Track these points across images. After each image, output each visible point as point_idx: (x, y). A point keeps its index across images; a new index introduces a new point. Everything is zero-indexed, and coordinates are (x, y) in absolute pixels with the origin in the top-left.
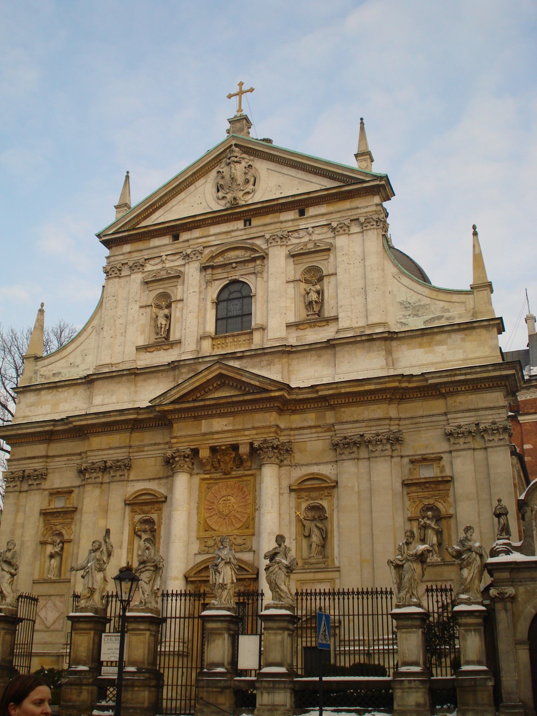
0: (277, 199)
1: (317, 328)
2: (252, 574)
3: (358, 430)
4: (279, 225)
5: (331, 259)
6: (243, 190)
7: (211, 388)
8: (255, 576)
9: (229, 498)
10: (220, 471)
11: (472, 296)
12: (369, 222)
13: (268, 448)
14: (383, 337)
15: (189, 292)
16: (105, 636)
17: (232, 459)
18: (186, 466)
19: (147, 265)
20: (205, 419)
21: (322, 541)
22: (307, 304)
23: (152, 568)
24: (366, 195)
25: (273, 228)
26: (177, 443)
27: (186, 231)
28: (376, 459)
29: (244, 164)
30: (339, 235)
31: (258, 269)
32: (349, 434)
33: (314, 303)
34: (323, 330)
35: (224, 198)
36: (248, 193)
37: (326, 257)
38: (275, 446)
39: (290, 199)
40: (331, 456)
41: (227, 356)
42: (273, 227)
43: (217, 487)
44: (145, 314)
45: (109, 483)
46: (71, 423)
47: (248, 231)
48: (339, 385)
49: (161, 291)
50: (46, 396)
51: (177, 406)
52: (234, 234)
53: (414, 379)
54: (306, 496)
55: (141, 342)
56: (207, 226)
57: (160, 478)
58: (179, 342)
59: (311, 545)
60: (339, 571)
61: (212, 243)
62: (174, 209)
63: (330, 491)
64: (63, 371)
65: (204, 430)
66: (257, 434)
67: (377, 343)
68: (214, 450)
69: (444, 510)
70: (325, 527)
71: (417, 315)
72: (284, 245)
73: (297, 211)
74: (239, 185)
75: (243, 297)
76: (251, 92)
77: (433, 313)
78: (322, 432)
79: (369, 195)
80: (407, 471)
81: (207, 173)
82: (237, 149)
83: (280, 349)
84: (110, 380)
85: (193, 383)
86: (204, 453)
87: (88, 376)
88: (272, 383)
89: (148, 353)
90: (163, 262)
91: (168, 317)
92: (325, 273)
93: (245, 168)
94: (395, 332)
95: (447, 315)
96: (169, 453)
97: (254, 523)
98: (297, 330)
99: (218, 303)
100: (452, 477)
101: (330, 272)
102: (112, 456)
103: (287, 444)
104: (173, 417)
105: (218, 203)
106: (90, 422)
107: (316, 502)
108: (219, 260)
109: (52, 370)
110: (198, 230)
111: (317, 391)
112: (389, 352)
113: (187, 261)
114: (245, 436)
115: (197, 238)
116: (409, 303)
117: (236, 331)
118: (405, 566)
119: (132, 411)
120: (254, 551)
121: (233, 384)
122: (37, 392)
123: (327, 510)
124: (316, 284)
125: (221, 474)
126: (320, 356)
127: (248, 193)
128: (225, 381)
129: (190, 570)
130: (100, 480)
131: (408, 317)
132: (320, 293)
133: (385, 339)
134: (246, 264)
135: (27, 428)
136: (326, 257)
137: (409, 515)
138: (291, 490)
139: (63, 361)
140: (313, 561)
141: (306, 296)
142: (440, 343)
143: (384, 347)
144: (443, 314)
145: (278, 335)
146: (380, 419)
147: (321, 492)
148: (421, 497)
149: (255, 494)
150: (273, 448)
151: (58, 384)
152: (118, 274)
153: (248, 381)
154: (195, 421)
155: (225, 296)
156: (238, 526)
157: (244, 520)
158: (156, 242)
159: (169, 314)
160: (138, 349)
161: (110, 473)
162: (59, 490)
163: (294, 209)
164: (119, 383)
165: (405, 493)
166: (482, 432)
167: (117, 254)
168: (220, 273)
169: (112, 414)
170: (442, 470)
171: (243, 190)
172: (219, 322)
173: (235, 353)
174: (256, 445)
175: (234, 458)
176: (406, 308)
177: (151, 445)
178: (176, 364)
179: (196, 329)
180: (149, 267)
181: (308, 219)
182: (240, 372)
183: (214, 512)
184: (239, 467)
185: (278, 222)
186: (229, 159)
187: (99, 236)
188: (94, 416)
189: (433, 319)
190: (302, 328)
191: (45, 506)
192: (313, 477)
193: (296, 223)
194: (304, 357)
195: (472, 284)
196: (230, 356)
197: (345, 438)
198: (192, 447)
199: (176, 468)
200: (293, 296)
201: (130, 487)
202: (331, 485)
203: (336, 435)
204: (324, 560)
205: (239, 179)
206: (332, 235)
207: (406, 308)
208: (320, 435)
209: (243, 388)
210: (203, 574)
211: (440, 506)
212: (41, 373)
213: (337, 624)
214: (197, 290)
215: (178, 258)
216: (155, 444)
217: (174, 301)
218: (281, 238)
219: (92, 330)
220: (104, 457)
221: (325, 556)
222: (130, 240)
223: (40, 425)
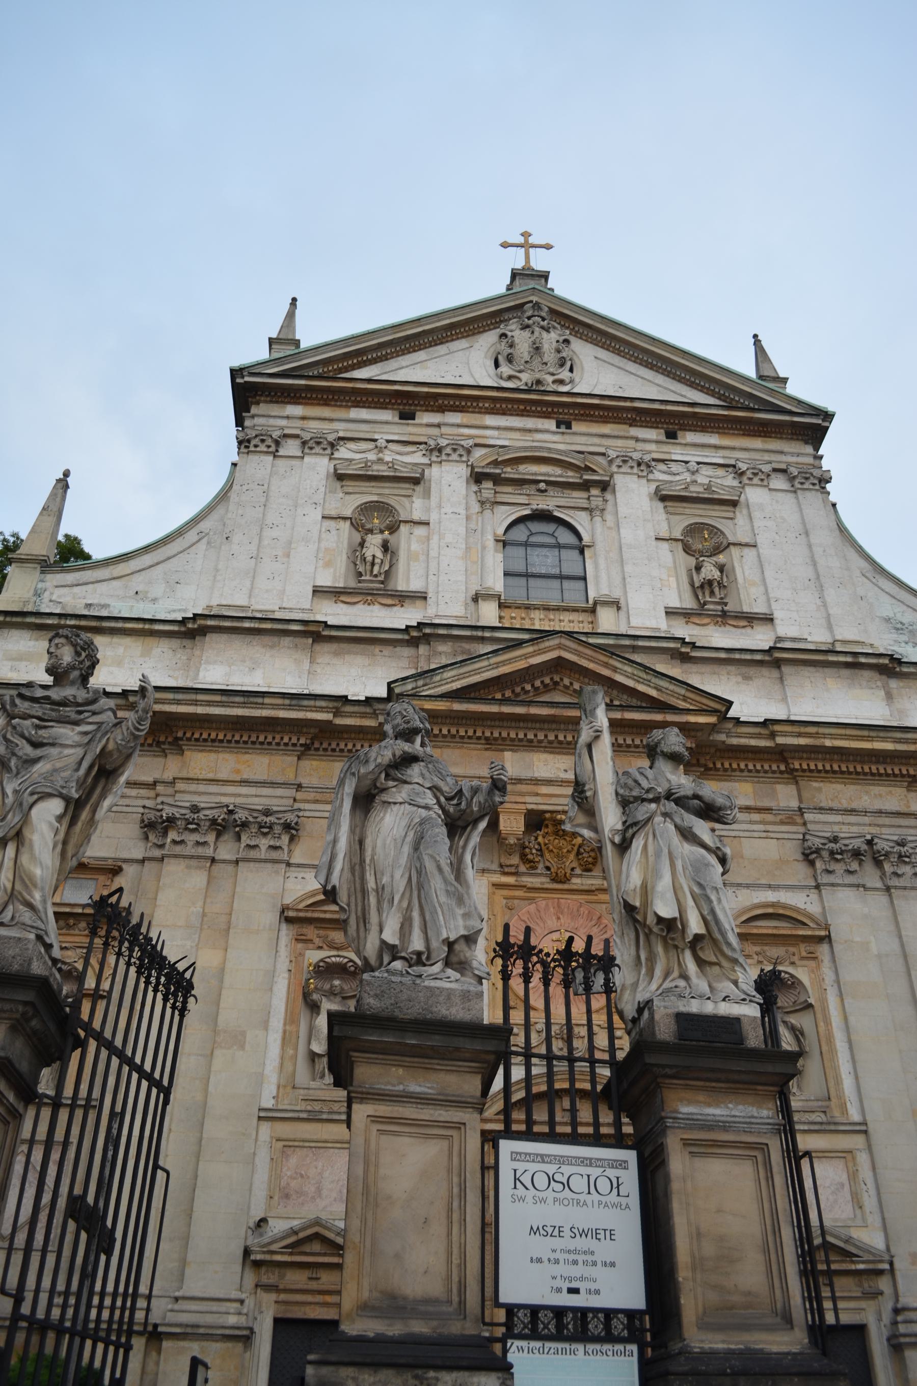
1: (728, 628)
3: (855, 829)
4: (631, 443)
7: (528, 687)
10: (541, 869)
15: (443, 511)
17: (576, 848)
19: (342, 449)
20: (511, 750)
22: (697, 584)
24: (792, 439)
25: (620, 445)
27: (433, 411)
28: (906, 893)
29: (554, 336)
30: (753, 485)
31: (596, 502)
33: (716, 584)
34: (742, 634)
35: (510, 378)
37: (731, 515)
39: (656, 406)
40: (800, 873)
42: (619, 443)
43: (532, 907)
44: (334, 532)
47: (568, 438)
48: (822, 730)
49: (375, 498)
51: (457, 706)
55: (326, 580)
60: (865, 1132)
61: (492, 442)
63: (812, 949)
67: (867, 674)
73: (662, 431)
74: (546, 364)
79: (798, 439)
81: (474, 334)
83: (672, 645)
84: (249, 638)
90: (380, 450)
92: (731, 539)
98: (687, 623)
106: (200, 710)
108: (509, 472)
110: (459, 414)
111: (773, 735)
112: (889, 696)
113: (434, 459)
115: (459, 426)
116: (901, 623)
119: (323, 703)
125: (544, 879)
126: (747, 678)
127: (561, 382)
130: (209, 852)
131: (903, 645)
133: (883, 670)
136: (731, 515)
141: (694, 571)
147: (792, 949)
151: (106, 624)
152: (273, 449)
153: (630, 683)
154: (486, 749)
160: (318, 592)
163: (657, 428)
164: (272, 647)
167: (273, 414)
168: (508, 494)
169: (267, 700)
175: (580, 846)
176: (898, 629)
178: (427, 631)
180: (343, 452)
181: (688, 448)
182: (612, 662)
184: (589, 870)
185: (632, 438)
186: (529, 318)
187: (235, 373)
188: (218, 698)
190: (698, 622)
193: (665, 448)
194: (714, 673)
197: (835, 840)
200: (671, 565)
201: (292, 879)
202: (817, 933)
206: (735, 483)
207: (898, 629)
214: (463, 512)
215: (415, 452)
217: (406, 522)
219: (196, 538)
220: (225, 800)
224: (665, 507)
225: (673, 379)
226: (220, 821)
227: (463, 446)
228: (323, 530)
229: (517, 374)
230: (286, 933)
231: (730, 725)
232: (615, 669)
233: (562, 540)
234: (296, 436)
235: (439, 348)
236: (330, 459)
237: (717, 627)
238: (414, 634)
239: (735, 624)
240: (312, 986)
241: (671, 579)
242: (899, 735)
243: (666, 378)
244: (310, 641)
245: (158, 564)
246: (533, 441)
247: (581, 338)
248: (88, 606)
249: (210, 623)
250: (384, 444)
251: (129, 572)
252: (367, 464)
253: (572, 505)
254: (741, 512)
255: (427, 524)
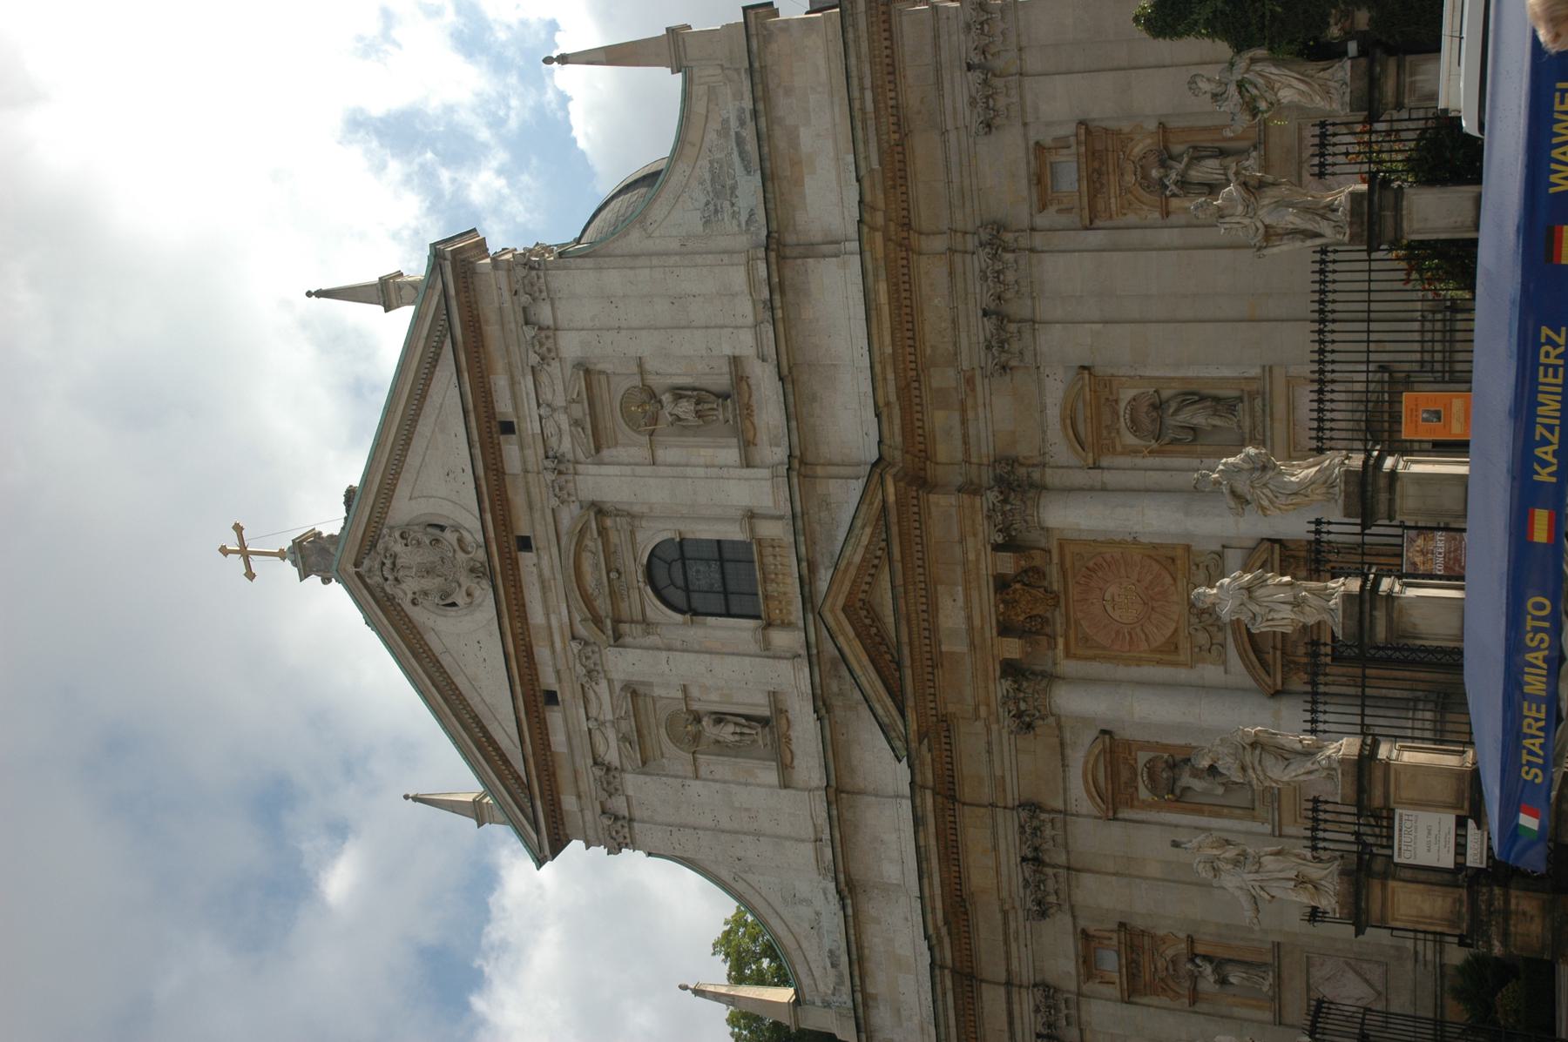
0: (476, 479)
2: (1273, 553)
5: (608, 367)
6: (454, 551)
7: (874, 630)
8: (1277, 546)
9: (1107, 596)
10: (1048, 615)
11: (695, 70)
12: (532, 285)
13: (1004, 513)
14: (778, 263)
16: (1400, 856)
18: (1037, 687)
19: (607, 759)
21: (1208, 404)
23: (1257, 752)
24: (474, 290)
25: (537, 490)
26: (988, 705)
27: (537, 674)
29: (398, 548)
30: (557, 349)
32: (982, 339)
35: (469, 594)
36: (460, 540)
38: (1001, 498)
39: (477, 451)
41: (807, 594)
42: (535, 491)
45: (1068, 852)
46: (936, 928)
48: (877, 359)
49: (663, 731)
50: (879, 983)
51: (910, 703)
52: (547, 573)
53: (868, 198)
54: (1110, 433)
55: (772, 777)
56: (528, 629)
57: (1062, 744)
58: (774, 696)
59: (1214, 426)
61: (566, 619)
62: (488, 700)
64: (828, 944)
65: (961, 647)
66: (975, 535)
68: (1005, 630)
69: (1149, 141)
70: (1176, 396)
71: (733, 188)
72: (574, 468)
73: (502, 437)
74: (442, 559)
75: (683, 558)
76: (242, 529)
77: (730, 154)
78: (975, 397)
80: (1064, 220)
81: (414, 627)
82: (366, 562)
85: (862, 667)
86: (1013, 648)
87: (839, 892)
88: (867, 501)
89: (796, 763)
90: (603, 723)
91: (720, 718)
92: (637, 381)
93: (406, 545)
94: (768, 236)
95: (734, 124)
96: (1008, 722)
97: (1162, 546)
99: (691, 611)
100: (1081, 123)
101: (635, 369)
102: (1010, 846)
103: (998, 471)
104: (934, 712)
105: (480, 605)
106: (938, 891)
107: (1122, 413)
109: (825, 969)
110: (535, 649)
112: (811, 250)
113: (602, 675)
114: (978, 560)
115: (553, 651)
116: (707, 204)
117: (755, 575)
118: (1267, 221)
119: (918, 801)
120: (1224, 547)
121: (866, 583)
122: (871, 1003)
123: (1142, 390)
124: (660, 402)
125: (1057, 613)
127: (460, 540)
128: (860, 600)
129: (1260, 685)
131: (735, 208)
132: (678, 393)
134: (612, 549)
135: (947, 1027)
136: (603, 378)
137: (1157, 215)
138: (1096, 467)
139: (805, 945)
140: (1247, 423)
142: (794, 141)
143: (799, 261)
144: (732, 133)
145: (767, 486)
146: (951, 274)
147: (1103, 400)
148: (1121, 190)
149: (1102, 542)
150: (1005, 501)
151: (854, 957)
154: (942, 666)
155: (678, 597)
156: (1168, 580)
157: (1156, 567)
158: (558, 740)
159: (713, 717)
160: (785, 784)
161: (1047, 850)
162: (1081, 961)
163: (499, 444)
165: (1108, 223)
166: (985, 58)
169: (922, 843)
170: (1061, 144)
171: (454, 551)
172: (734, 610)
173: (800, 577)
174: (1000, 539)
175: (1025, 584)
177: (991, 761)
178: (820, 703)
179: (747, 660)
180: (612, 756)
183: (1138, 630)
184: (1044, 575)
185: (525, 477)
186: (386, 579)
188: (926, 881)
189: (742, 154)
190: (752, 433)
191: (1114, 991)
192: (1070, 421)
195: (669, 69)
196: (807, 589)
197: (989, 347)
198: (998, 673)
199: (1042, 708)
202: (1087, 381)
203: (982, 368)
204: (1246, 399)
205: (432, 559)
206: (556, 364)
207: (716, 211)
208: (980, 401)
209: (876, 562)
210: (1269, 658)
211: (1138, 149)
212: (830, 992)
213: (1386, 376)
214: (664, 654)
216: (989, 752)
218: (560, 473)
220: (1012, 862)
221: (1236, 398)
222: (552, 795)
223: (940, 997)
224: (609, 447)
225: (419, 415)
226: (1035, 868)
227: (580, 651)
228: (710, 777)
229: (464, 589)
230: (1125, 813)
231: (885, 448)
232: (849, 564)
233: (676, 555)
234: (601, 803)
235: (443, 663)
236: (623, 770)
237: (755, 413)
238: (823, 712)
239: (747, 395)
240: (1170, 796)
241: (702, 453)
242: (870, 278)
243: (420, 422)
244: (843, 795)
245: (777, 913)
246: (555, 579)
247: (386, 513)
248: (834, 965)
249: (842, 877)
250: (592, 724)
251: (790, 935)
252: (624, 738)
253: (630, 546)
254: (595, 364)
255: (685, 689)
